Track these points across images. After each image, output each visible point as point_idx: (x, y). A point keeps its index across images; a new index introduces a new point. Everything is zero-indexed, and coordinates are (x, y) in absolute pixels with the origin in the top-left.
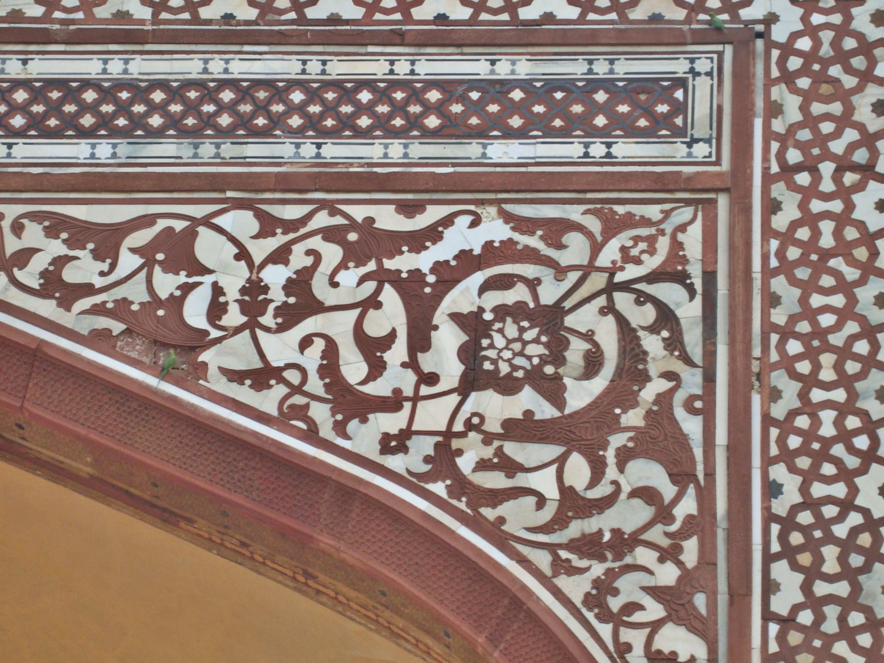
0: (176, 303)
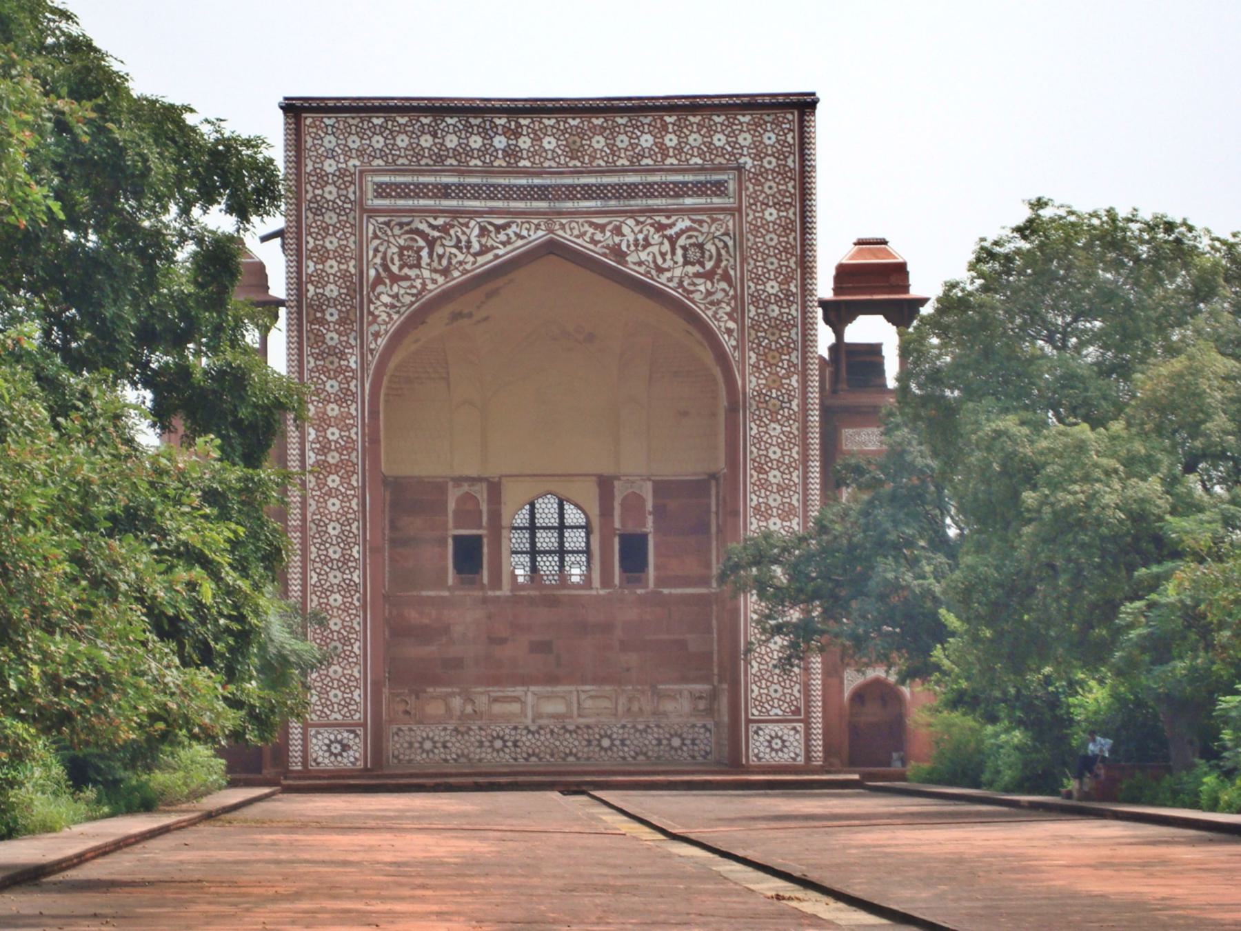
0: (619, 245)
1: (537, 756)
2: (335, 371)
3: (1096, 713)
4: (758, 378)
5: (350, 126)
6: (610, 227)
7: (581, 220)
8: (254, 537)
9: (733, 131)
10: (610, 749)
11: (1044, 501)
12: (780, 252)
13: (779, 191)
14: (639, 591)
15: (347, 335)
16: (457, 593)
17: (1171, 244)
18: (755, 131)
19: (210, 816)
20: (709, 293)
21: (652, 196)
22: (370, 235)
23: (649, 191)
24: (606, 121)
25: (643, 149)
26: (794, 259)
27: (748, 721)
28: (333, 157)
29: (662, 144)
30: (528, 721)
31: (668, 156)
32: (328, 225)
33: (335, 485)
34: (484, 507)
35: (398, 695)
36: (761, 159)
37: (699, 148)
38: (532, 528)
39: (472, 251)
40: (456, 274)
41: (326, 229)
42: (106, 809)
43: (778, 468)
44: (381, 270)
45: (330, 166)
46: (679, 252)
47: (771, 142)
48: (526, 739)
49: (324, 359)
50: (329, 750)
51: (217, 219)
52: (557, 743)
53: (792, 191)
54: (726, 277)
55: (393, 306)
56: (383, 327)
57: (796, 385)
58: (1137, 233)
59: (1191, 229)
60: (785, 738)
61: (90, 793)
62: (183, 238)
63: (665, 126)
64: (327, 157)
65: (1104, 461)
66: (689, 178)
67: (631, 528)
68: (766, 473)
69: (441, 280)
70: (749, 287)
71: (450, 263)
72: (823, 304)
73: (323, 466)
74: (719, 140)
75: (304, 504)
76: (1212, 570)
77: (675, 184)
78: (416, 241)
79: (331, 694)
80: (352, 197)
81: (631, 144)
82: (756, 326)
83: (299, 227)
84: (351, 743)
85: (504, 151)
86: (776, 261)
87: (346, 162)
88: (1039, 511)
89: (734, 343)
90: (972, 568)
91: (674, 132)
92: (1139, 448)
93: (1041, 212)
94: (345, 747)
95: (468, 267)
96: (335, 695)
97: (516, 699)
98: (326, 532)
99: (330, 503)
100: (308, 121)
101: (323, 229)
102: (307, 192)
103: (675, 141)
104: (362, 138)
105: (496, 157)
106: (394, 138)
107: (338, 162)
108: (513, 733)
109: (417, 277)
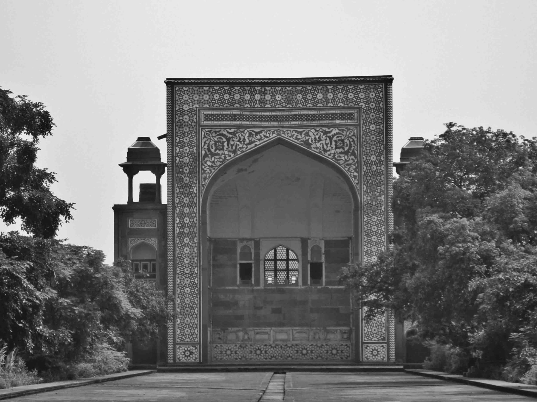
0: (308, 140)
1: (275, 357)
2: (188, 194)
3: (478, 340)
4: (367, 197)
5: (194, 91)
6: (304, 133)
7: (292, 130)
8: (41, 267)
9: (357, 92)
10: (306, 354)
11: (447, 250)
12: (377, 143)
13: (376, 117)
14: (319, 287)
15: (193, 178)
16: (241, 288)
17: (505, 141)
18: (366, 92)
19: (97, 382)
20: (346, 161)
21: (322, 119)
22: (203, 136)
23: (321, 117)
24: (303, 88)
25: (318, 100)
26: (383, 146)
27: (363, 343)
28: (187, 104)
29: (327, 97)
30: (271, 342)
31: (329, 102)
32: (185, 132)
33: (187, 242)
34: (253, 251)
35: (216, 331)
36: (369, 104)
37: (342, 99)
38: (275, 260)
39: (246, 143)
40: (239, 152)
41: (184, 134)
42: (42, 379)
43: (376, 235)
44: (207, 151)
45: (186, 107)
46: (334, 143)
47: (373, 97)
48: (270, 350)
49: (183, 189)
50: (184, 354)
51: (25, 137)
52: (284, 352)
53: (382, 117)
54: (353, 154)
55: (212, 166)
56: (208, 175)
57: (383, 200)
58: (491, 137)
59: (514, 136)
60: (379, 350)
61: (35, 372)
62: (12, 145)
63: (328, 90)
64: (185, 104)
65: (472, 234)
66: (338, 112)
67: (315, 260)
68: (371, 237)
69: (232, 155)
70: (363, 158)
71: (236, 148)
72: (395, 165)
73: (181, 234)
74: (351, 96)
75: (174, 250)
76: (485, 281)
77: (332, 114)
78: (222, 139)
79: (185, 331)
80: (195, 120)
81: (313, 98)
82: (366, 174)
83: (173, 133)
84: (194, 351)
85: (259, 100)
86: (375, 147)
87: (192, 106)
88: (444, 254)
89: (357, 182)
90: (418, 279)
91: (332, 92)
92: (487, 228)
93: (452, 129)
94: (191, 353)
95: (244, 150)
96: (187, 331)
97: (266, 333)
98: (183, 262)
99: (185, 250)
100: (177, 88)
101: (183, 134)
102: (176, 118)
103: (332, 96)
104: (200, 96)
105: (256, 103)
106: (213, 96)
107: (189, 106)
108: (265, 347)
109: (222, 154)
